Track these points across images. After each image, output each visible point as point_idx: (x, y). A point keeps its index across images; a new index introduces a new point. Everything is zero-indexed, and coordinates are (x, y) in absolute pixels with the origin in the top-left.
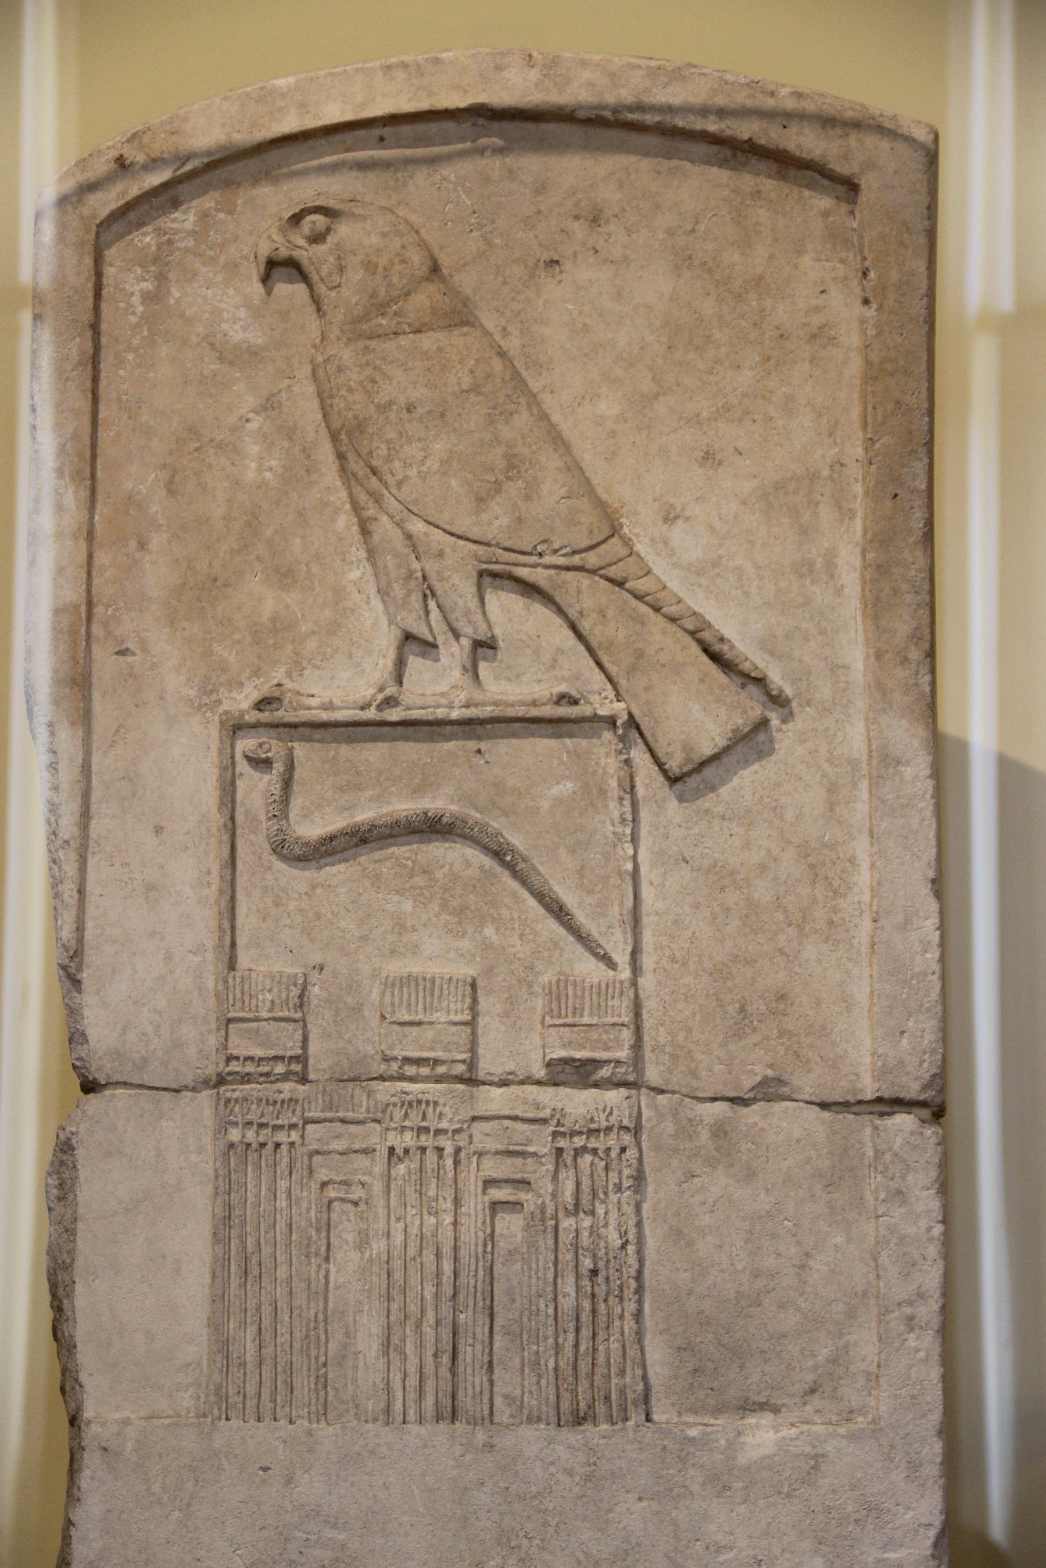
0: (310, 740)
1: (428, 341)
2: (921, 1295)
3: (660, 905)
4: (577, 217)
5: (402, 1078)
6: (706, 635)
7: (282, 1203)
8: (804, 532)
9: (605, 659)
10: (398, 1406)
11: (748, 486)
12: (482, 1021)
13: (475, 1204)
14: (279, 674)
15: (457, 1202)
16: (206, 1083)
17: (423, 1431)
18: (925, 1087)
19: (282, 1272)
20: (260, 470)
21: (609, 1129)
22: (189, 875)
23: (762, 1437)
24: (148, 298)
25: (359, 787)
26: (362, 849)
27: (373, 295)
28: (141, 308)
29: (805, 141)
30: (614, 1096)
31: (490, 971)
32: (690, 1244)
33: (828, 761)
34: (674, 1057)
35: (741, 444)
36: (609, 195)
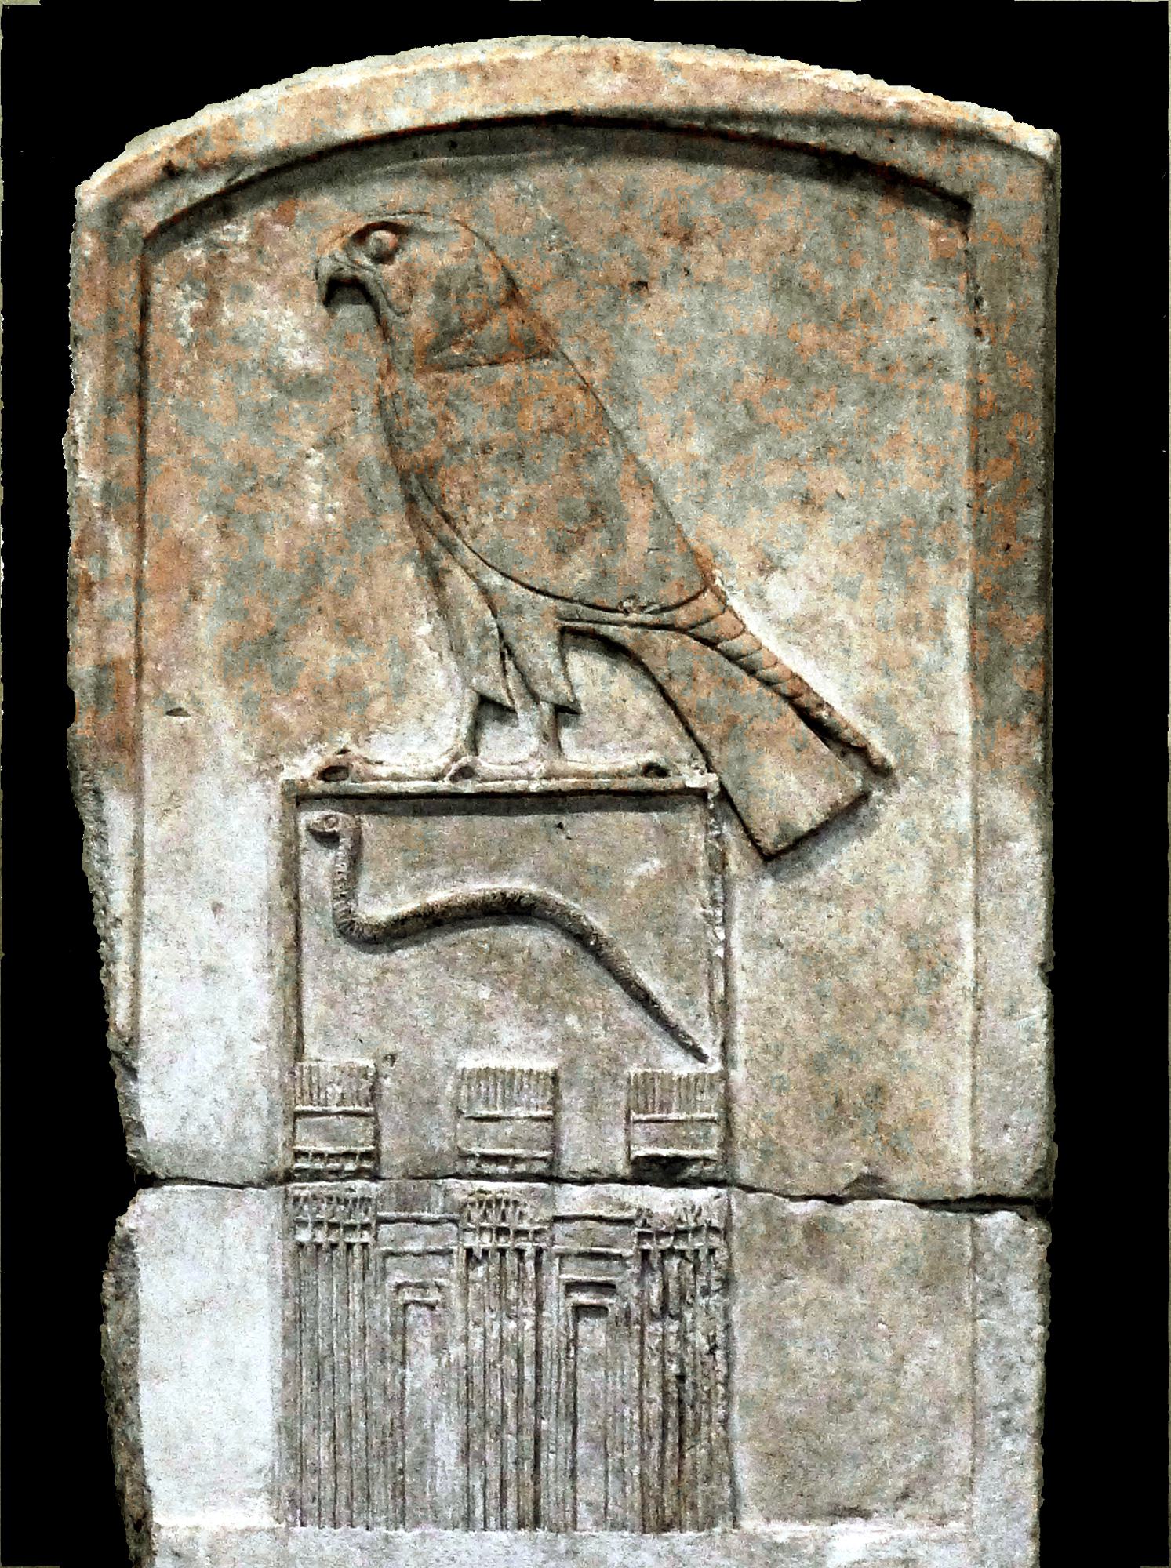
1: (506, 374)
2: (1019, 1398)
3: (752, 992)
4: (666, 235)
5: (479, 1176)
9: (694, 724)
10: (479, 1512)
11: (851, 533)
12: (564, 1116)
13: (557, 1308)
14: (345, 738)
15: (539, 1306)
16: (270, 1180)
18: (1028, 1183)
19: (357, 1377)
20: (322, 511)
21: (697, 1231)
22: (248, 956)
24: (197, 318)
25: (431, 864)
27: (444, 323)
28: (191, 330)
30: (702, 1196)
32: (782, 1348)
33: (936, 835)
34: (764, 1153)
35: (842, 488)
36: (704, 213)
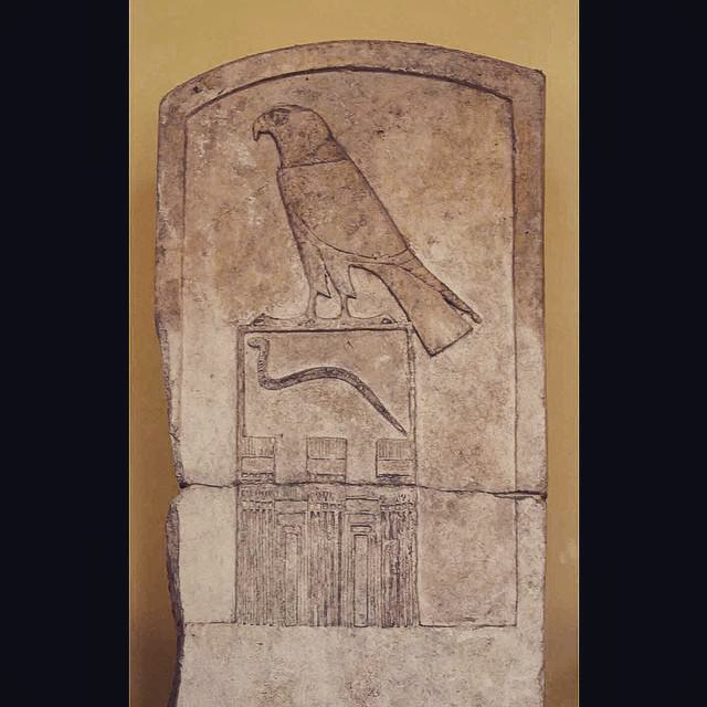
1: (326, 167)
3: (427, 409)
4: (390, 112)
6: (446, 293)
9: (402, 303)
10: (316, 619)
11: (465, 228)
12: (349, 459)
13: (347, 535)
14: (263, 310)
15: (340, 534)
24: (207, 147)
25: (297, 358)
28: (203, 152)
29: (488, 81)
30: (406, 491)
32: (438, 552)
34: (432, 473)
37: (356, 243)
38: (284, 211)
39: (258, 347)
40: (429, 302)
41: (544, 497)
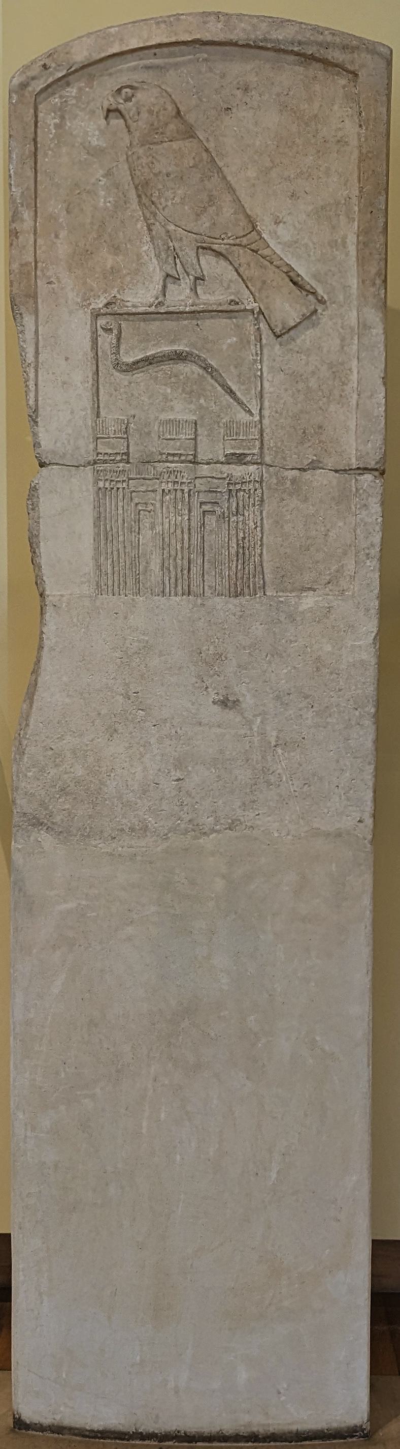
0: (128, 320)
1: (175, 145)
2: (372, 545)
3: (272, 389)
5: (167, 461)
6: (291, 274)
7: (120, 511)
8: (334, 227)
9: (249, 285)
11: (310, 208)
12: (199, 438)
13: (196, 512)
14: (114, 292)
16: (89, 463)
17: (178, 599)
18: (377, 463)
19: (121, 538)
20: (105, 202)
21: (250, 481)
22: (80, 377)
23: (309, 601)
24: (57, 126)
25: (148, 341)
26: (150, 367)
27: (152, 125)
29: (336, 55)
30: (252, 468)
31: (202, 418)
32: (282, 527)
33: (342, 327)
34: (276, 452)
35: (307, 189)
36: (253, 79)
37: (205, 224)
38: (134, 191)
39: (111, 329)
40: (274, 284)
41: (383, 473)
